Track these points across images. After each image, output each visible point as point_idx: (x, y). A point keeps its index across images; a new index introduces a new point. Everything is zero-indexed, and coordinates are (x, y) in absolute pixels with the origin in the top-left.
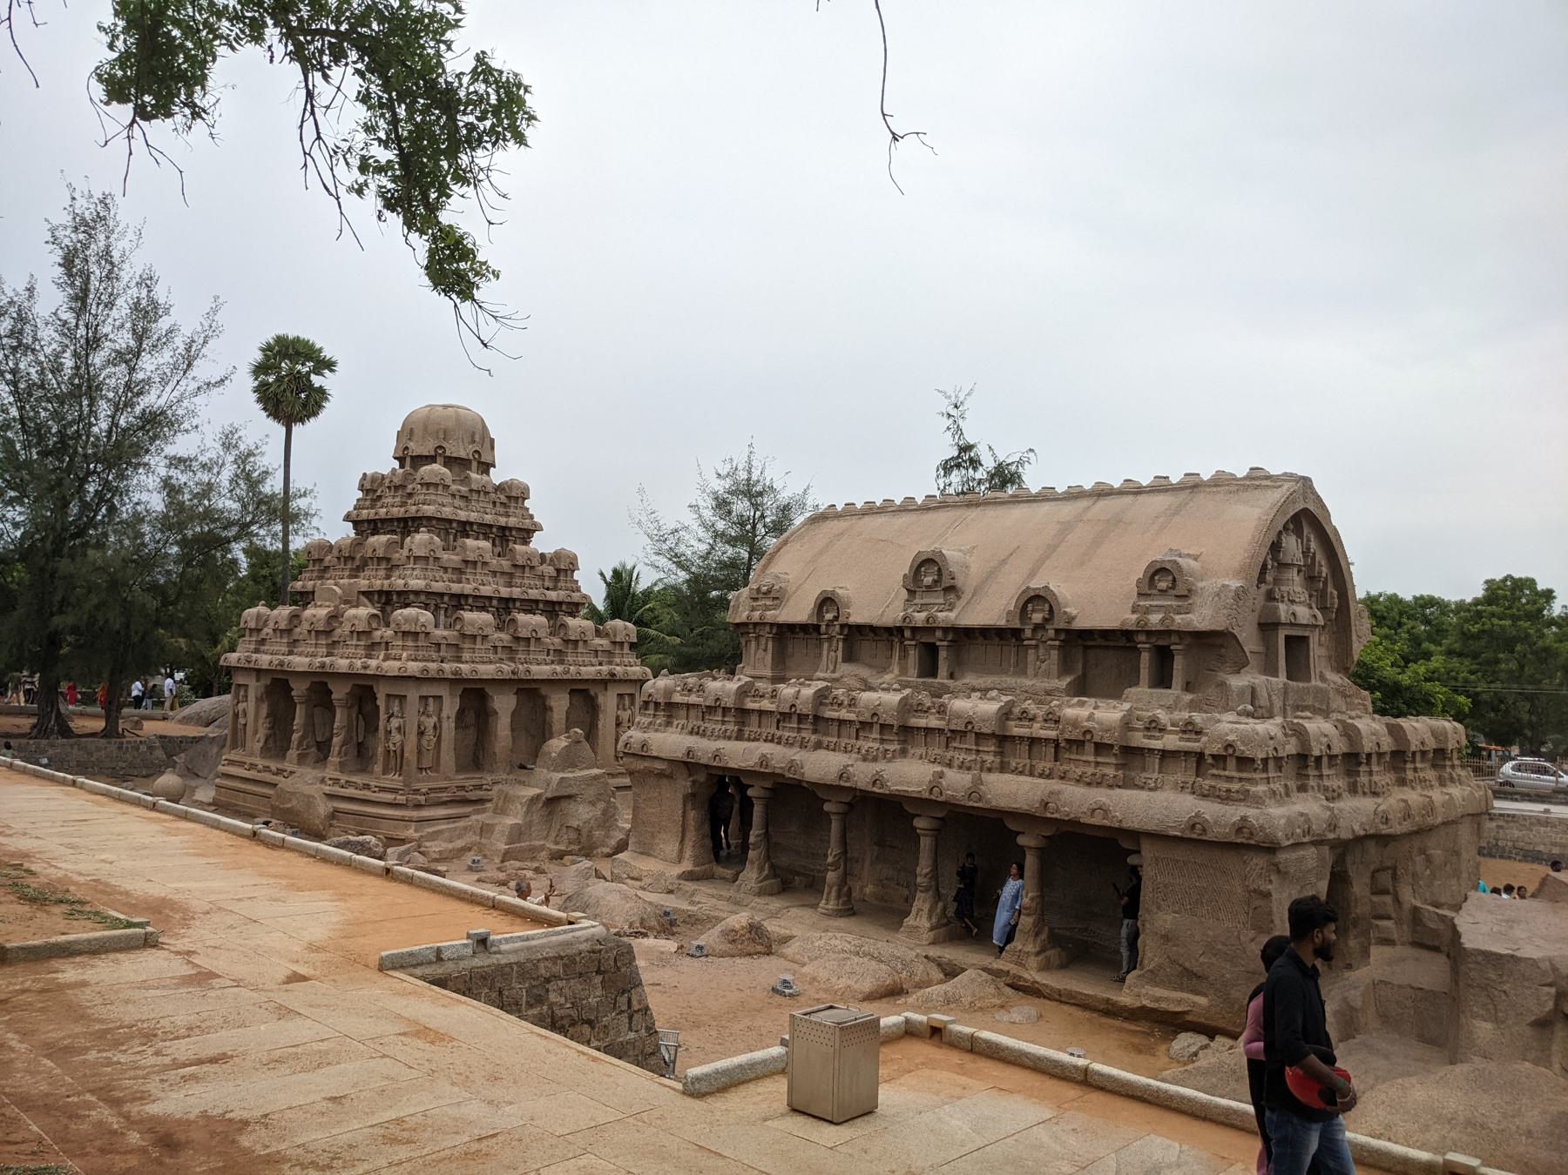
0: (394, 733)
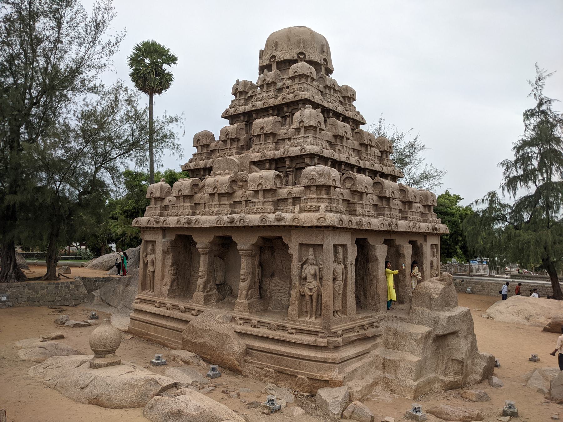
0: (310, 279)
